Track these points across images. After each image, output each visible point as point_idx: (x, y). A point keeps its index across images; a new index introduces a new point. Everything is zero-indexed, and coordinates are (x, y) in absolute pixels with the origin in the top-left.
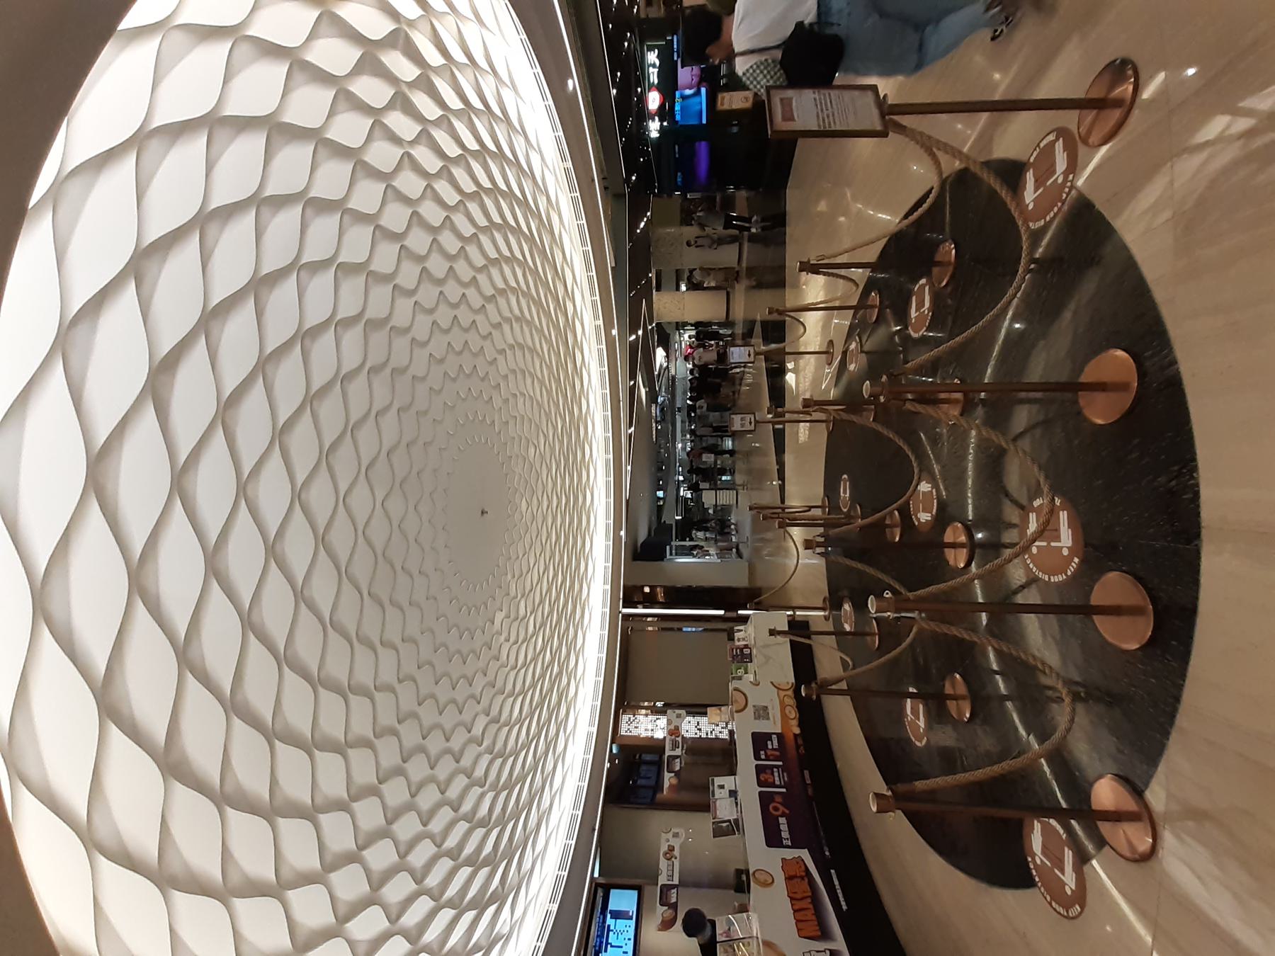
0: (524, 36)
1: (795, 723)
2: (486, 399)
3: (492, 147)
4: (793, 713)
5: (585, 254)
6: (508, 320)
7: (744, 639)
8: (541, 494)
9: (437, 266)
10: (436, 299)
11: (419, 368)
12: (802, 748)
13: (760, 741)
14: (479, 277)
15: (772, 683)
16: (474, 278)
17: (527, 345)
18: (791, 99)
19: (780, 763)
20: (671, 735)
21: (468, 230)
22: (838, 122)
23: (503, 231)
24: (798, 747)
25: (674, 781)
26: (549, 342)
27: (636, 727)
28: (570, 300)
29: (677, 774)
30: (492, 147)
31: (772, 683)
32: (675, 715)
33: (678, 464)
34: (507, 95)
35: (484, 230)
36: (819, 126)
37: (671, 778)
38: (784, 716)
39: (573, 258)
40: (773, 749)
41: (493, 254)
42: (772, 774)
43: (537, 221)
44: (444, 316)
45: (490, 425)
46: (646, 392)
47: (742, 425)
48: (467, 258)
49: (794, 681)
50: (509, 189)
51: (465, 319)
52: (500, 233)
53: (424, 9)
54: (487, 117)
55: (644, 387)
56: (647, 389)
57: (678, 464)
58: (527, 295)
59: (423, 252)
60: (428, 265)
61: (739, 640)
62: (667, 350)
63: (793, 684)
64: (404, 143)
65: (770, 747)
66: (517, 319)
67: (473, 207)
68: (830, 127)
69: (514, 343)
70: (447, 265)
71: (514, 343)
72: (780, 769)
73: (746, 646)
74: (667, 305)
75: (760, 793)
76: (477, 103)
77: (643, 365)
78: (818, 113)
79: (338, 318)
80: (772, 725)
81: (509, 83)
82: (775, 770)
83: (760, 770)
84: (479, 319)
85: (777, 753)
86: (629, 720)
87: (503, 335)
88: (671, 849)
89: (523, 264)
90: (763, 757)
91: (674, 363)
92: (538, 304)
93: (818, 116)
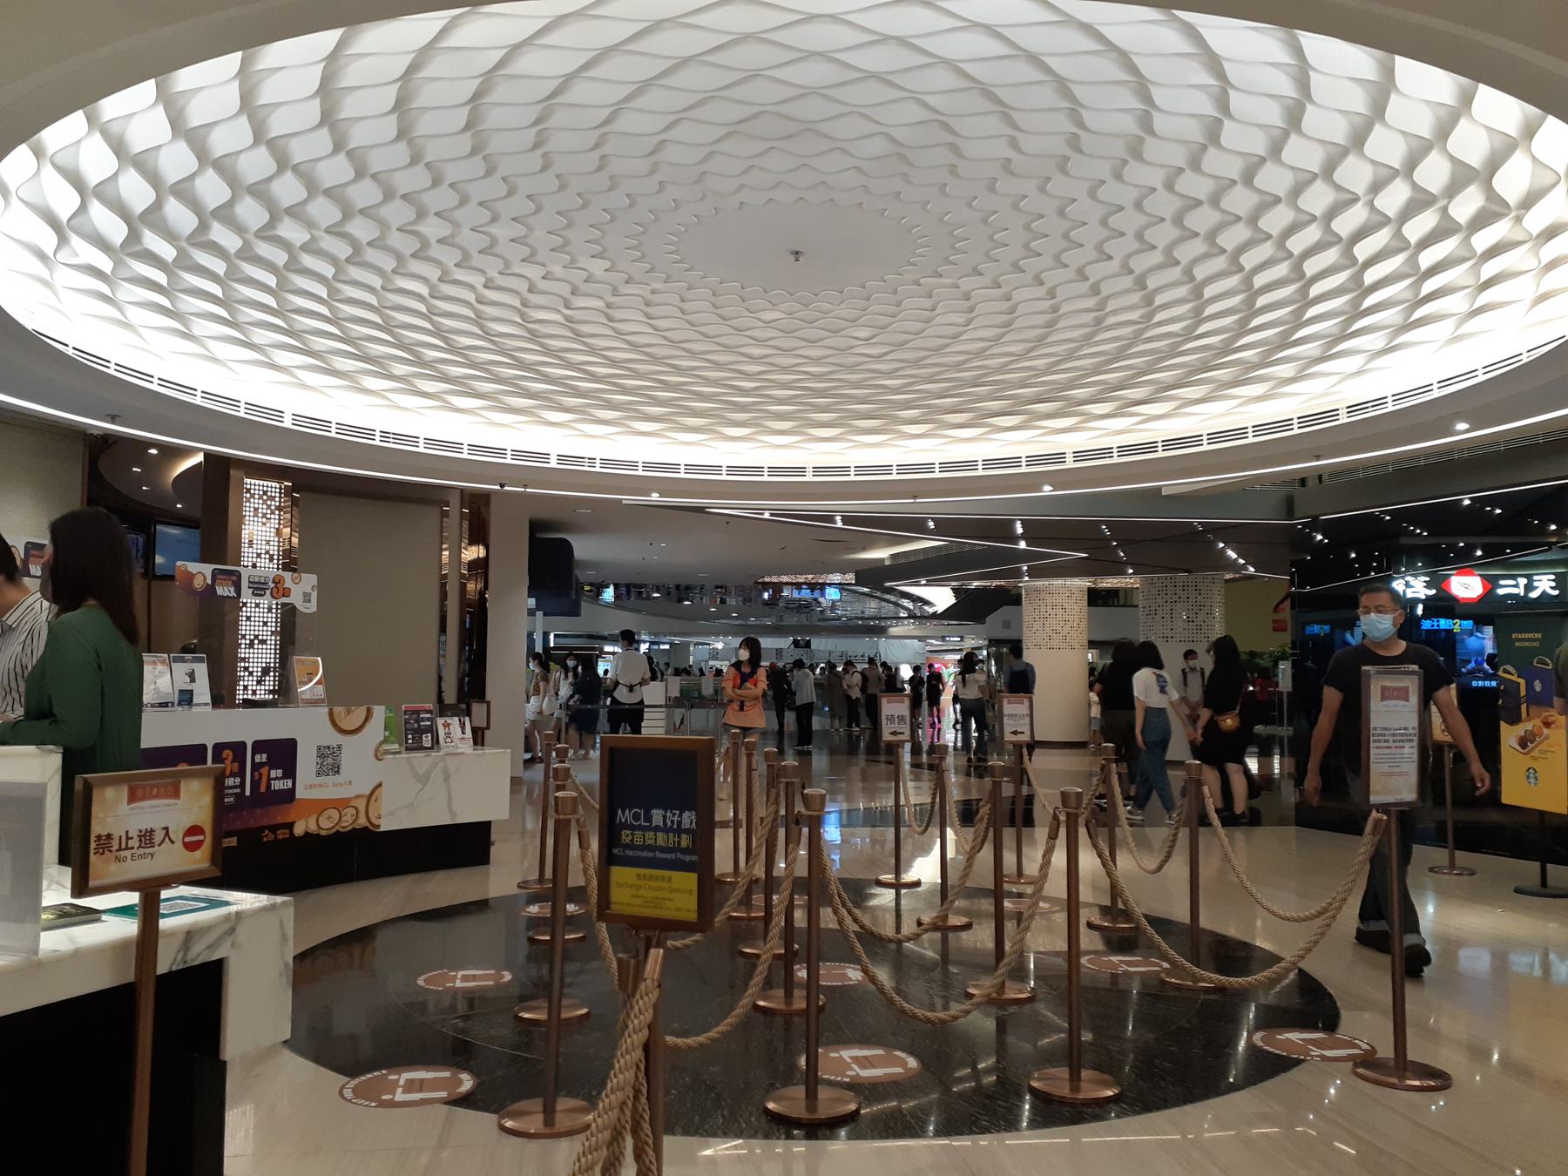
0: (1525, 359)
1: (313, 828)
2: (951, 258)
3: (1369, 302)
4: (327, 823)
5: (1195, 439)
6: (1101, 306)
8: (839, 361)
9: (1202, 219)
10: (1155, 213)
11: (1059, 186)
12: (272, 837)
13: (282, 753)
14: (1178, 269)
15: (380, 785)
16: (1178, 263)
17: (1050, 333)
18: (1406, 699)
19: (248, 793)
20: (274, 582)
21: (1249, 260)
22: (1380, 751)
23: (1245, 308)
24: (274, 828)
25: (198, 583)
26: (1048, 371)
27: (256, 509)
28: (1117, 409)
29: (210, 589)
30: (1369, 302)
31: (380, 785)
32: (309, 591)
33: (677, 640)
34: (1444, 329)
35: (1248, 281)
36: (1375, 729)
37: (205, 579)
38: (321, 806)
39: (1192, 417)
40: (269, 779)
41: (1209, 292)
43: (1256, 360)
44: (1129, 221)
45: (937, 272)
46: (882, 560)
47: (891, 719)
48: (1206, 256)
49: (382, 829)
50: (1306, 321)
51: (1117, 248)
52: (1240, 303)
53: (1539, 236)
54: (1412, 297)
55: (893, 556)
56: (887, 563)
57: (677, 640)
58: (1137, 338)
59: (1224, 204)
60: (1205, 209)
61: (447, 725)
62: (949, 614)
63: (378, 826)
64: (1372, 196)
65: (273, 774)
66: (1099, 321)
67: (1282, 270)
68: (1374, 741)
69: (1060, 313)
70: (1202, 230)
71: (1060, 313)
72: (238, 790)
73: (436, 741)
74: (1060, 612)
75: (204, 747)
76: (1429, 286)
77: (967, 548)
78: (1390, 729)
79: (1153, 112)
80: (308, 782)
81: (1458, 332)
82: (238, 780)
83: (238, 748)
84: (1114, 266)
85: (263, 789)
86: (272, 498)
87: (1078, 297)
89: (1188, 335)
90: (258, 758)
91: (917, 633)
92: (1120, 354)
93: (1385, 729)
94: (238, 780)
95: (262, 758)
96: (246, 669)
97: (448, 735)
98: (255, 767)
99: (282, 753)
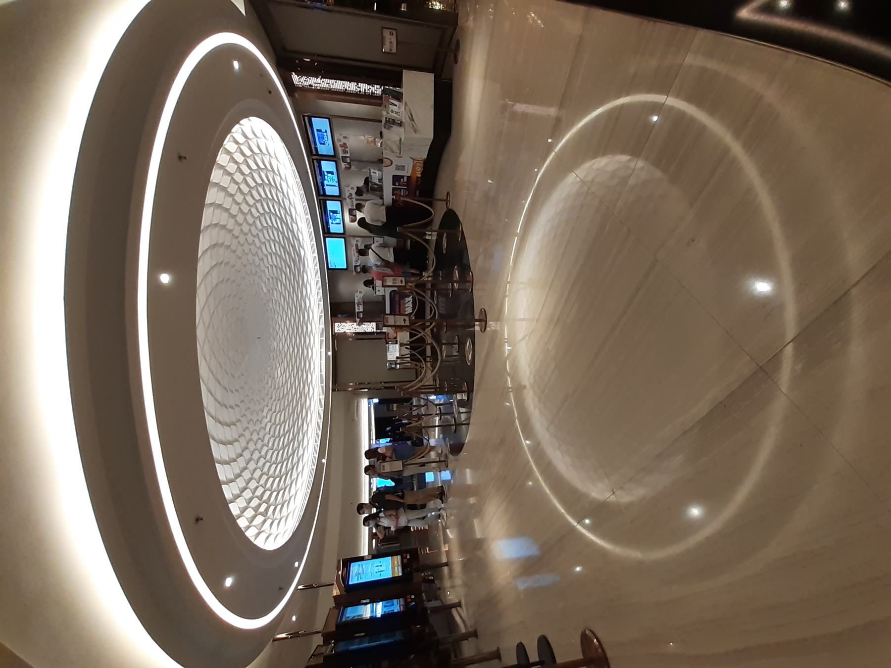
7: (397, 113)
19: (406, 187)
42: (401, 191)
80: (407, 172)
88: (351, 195)
90: (397, 185)
94: (402, 190)
95: (397, 184)
96: (368, 90)
97: (397, 113)
98: (399, 185)
99: (396, 179)
